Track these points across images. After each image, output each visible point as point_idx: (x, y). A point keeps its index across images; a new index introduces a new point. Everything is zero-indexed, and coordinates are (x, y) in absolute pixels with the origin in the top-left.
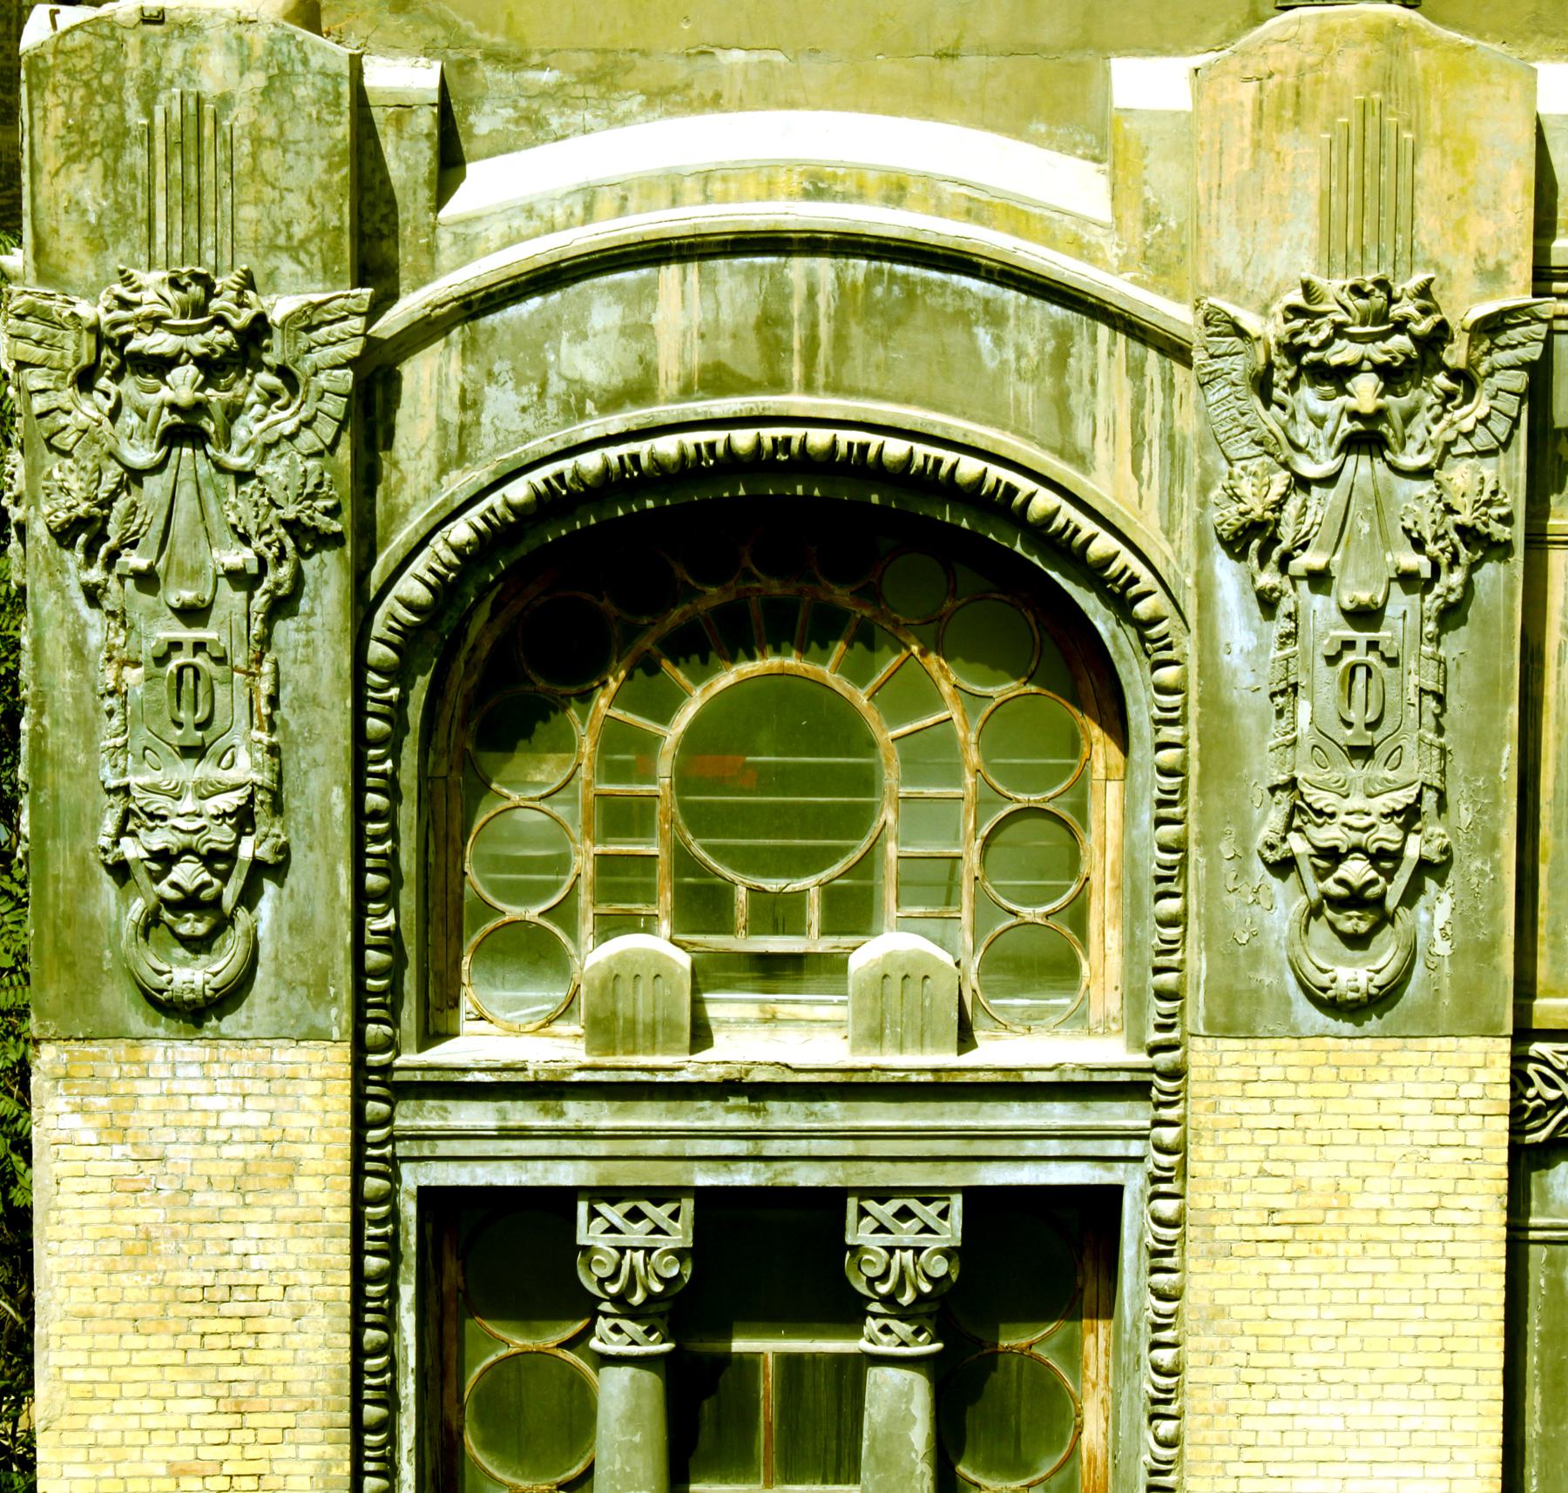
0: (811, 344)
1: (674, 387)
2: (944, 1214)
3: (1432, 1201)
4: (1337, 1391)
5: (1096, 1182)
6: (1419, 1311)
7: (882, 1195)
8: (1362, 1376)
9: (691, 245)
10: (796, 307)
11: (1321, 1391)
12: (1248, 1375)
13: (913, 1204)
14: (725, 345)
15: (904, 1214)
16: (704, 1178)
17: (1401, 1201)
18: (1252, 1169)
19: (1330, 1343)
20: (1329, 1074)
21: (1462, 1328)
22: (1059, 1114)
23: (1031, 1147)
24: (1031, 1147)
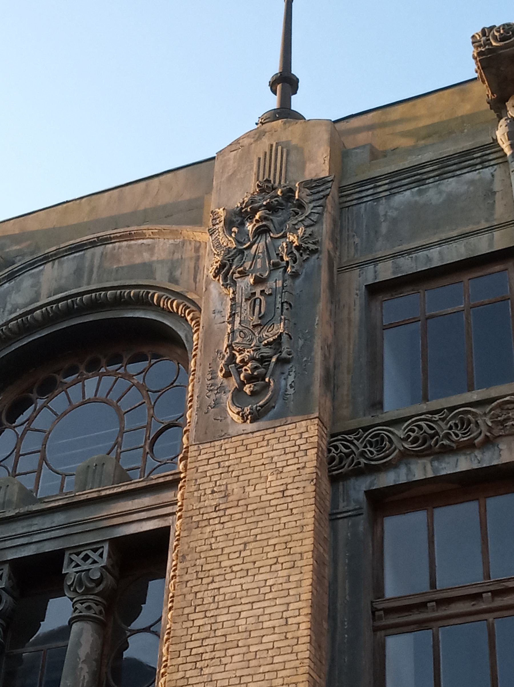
0: (91, 272)
1: (45, 296)
2: (101, 555)
3: (282, 488)
4: (239, 574)
5: (160, 526)
6: (277, 534)
7: (77, 549)
8: (250, 566)
9: (55, 255)
10: (87, 264)
11: (233, 575)
12: (201, 575)
13: (90, 553)
14: (63, 281)
15: (86, 558)
16: (11, 556)
17: (270, 490)
18: (209, 491)
19: (237, 555)
20: (242, 448)
21: (295, 537)
22: (146, 501)
23: (135, 517)
24: (135, 517)
